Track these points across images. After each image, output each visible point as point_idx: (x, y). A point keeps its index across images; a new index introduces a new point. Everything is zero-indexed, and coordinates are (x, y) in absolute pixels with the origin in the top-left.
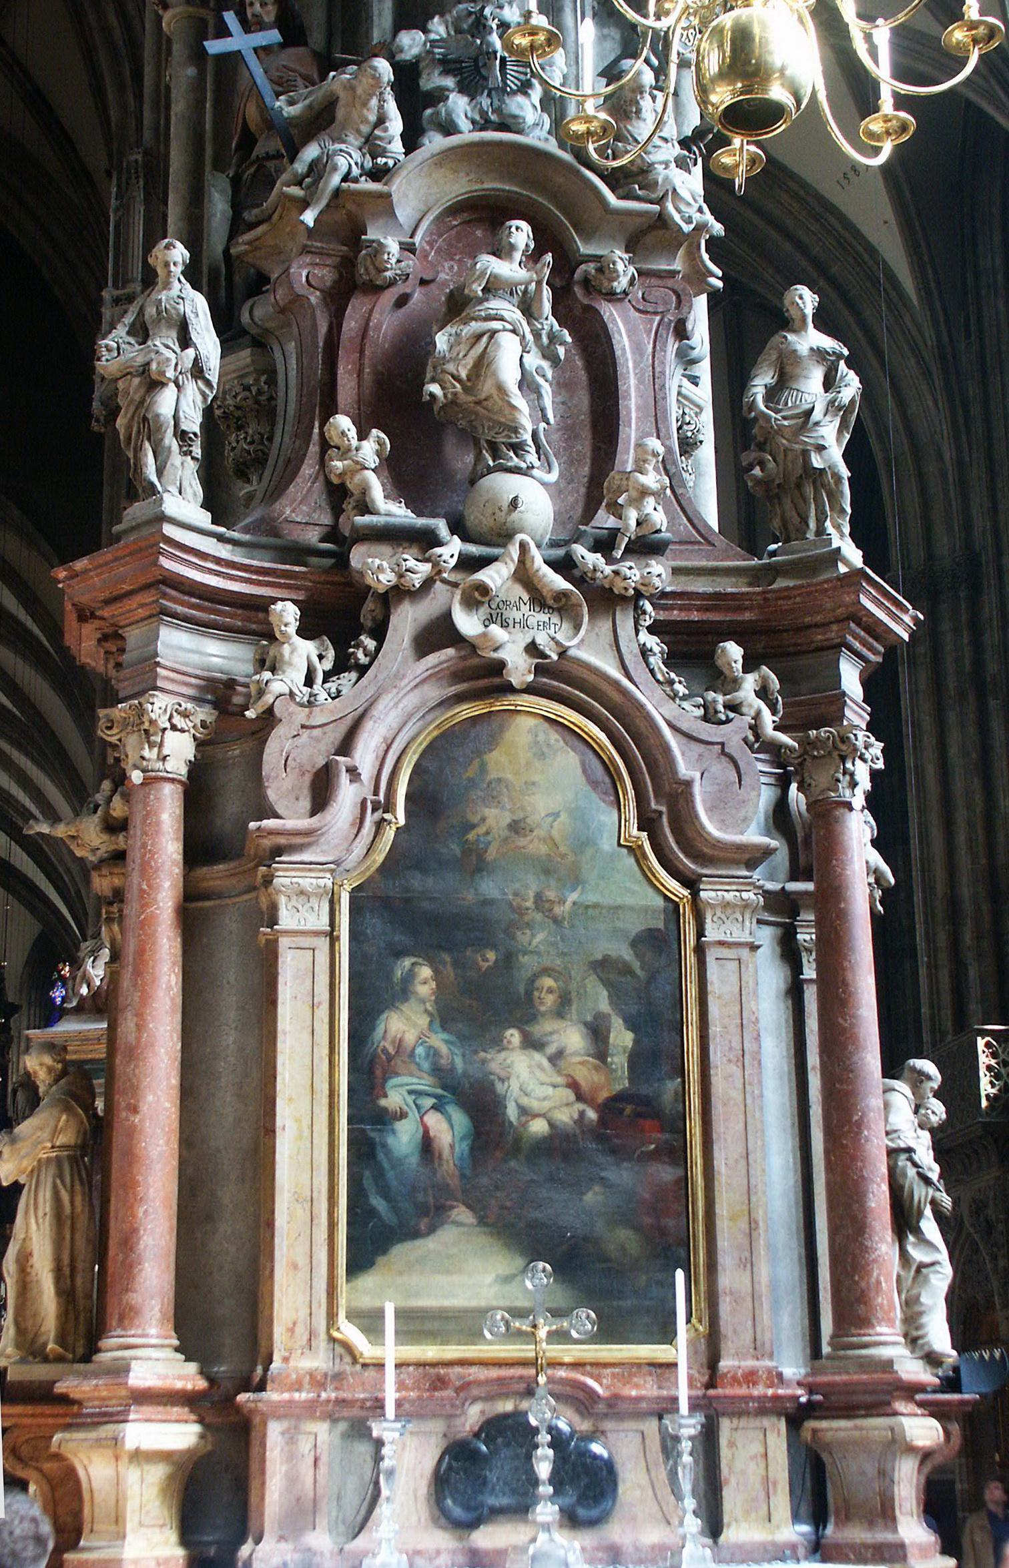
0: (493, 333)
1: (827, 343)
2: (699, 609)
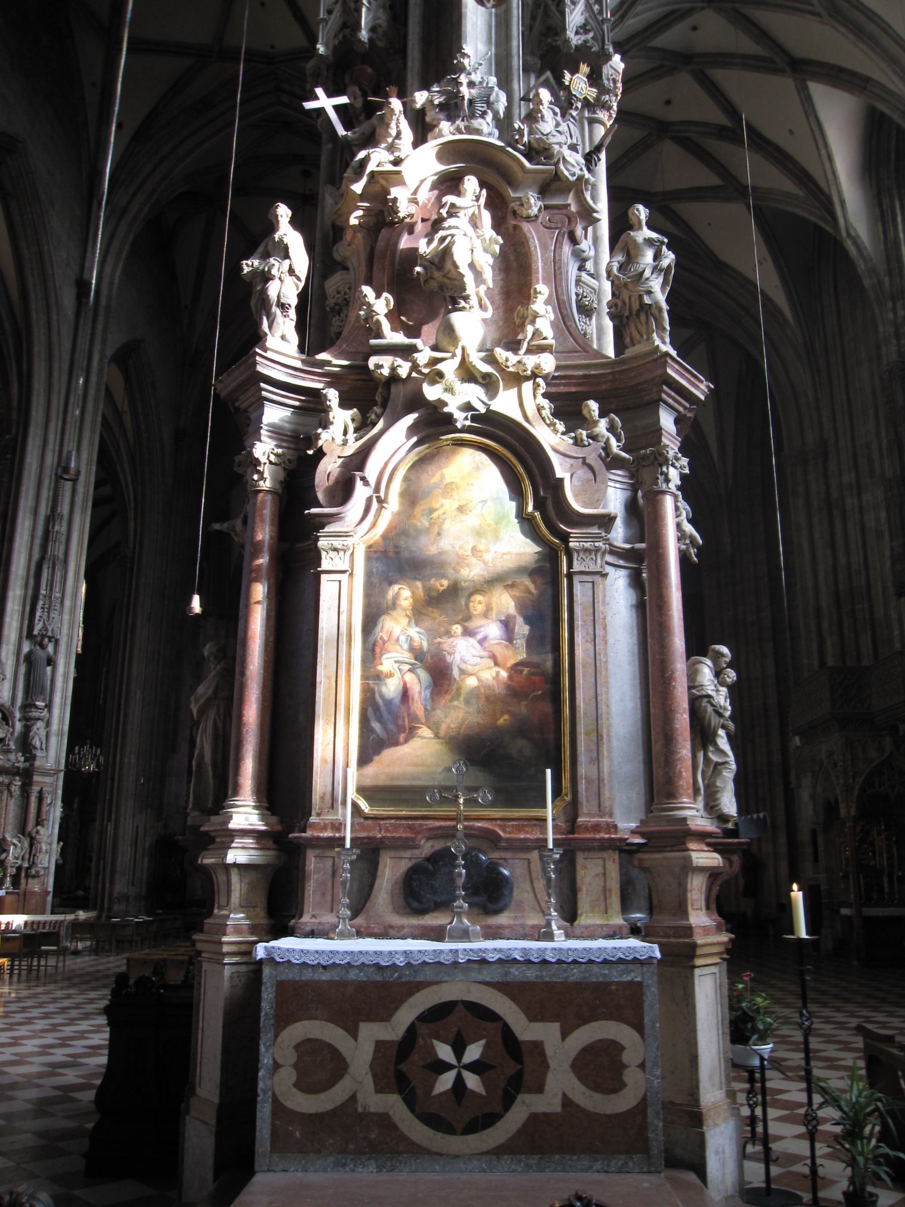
0: (453, 236)
1: (654, 235)
2: (575, 385)
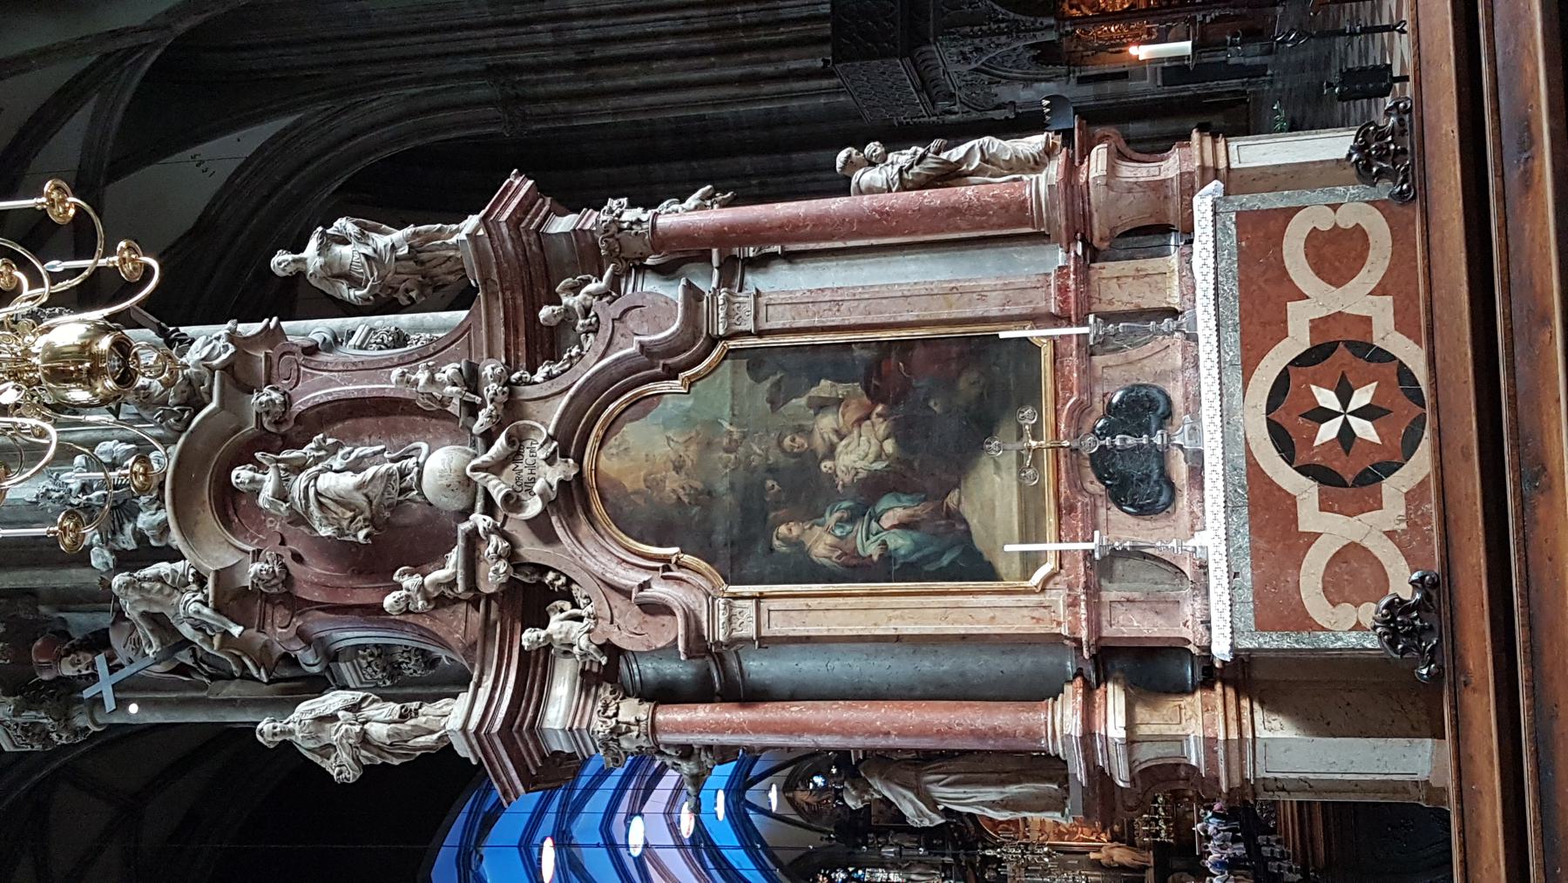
0: (317, 494)
1: (313, 243)
2: (517, 336)
